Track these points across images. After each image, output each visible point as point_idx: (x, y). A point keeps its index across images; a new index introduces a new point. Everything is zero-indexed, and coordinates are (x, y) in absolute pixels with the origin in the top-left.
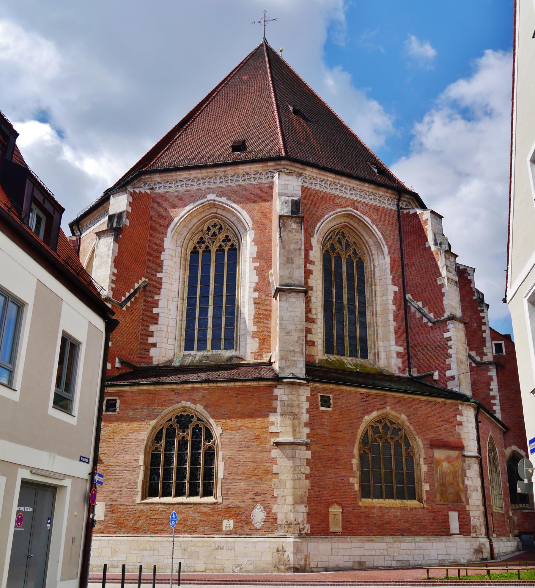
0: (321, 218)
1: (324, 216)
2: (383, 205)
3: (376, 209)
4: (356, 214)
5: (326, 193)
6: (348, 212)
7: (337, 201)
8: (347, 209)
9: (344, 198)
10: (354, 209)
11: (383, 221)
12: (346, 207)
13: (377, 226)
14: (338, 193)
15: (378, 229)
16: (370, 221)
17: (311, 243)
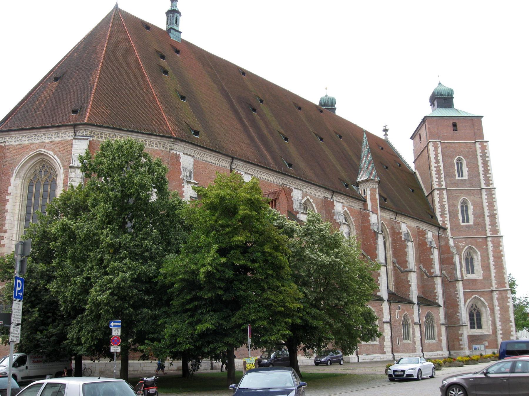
0: (19, 162)
1: (21, 160)
2: (65, 139)
3: (58, 144)
4: (44, 152)
5: (24, 144)
6: (38, 152)
7: (32, 147)
8: (38, 150)
9: (36, 143)
10: (43, 149)
11: (63, 150)
12: (37, 149)
13: (57, 156)
14: (33, 141)
15: (58, 157)
16: (53, 154)
17: (10, 181)
